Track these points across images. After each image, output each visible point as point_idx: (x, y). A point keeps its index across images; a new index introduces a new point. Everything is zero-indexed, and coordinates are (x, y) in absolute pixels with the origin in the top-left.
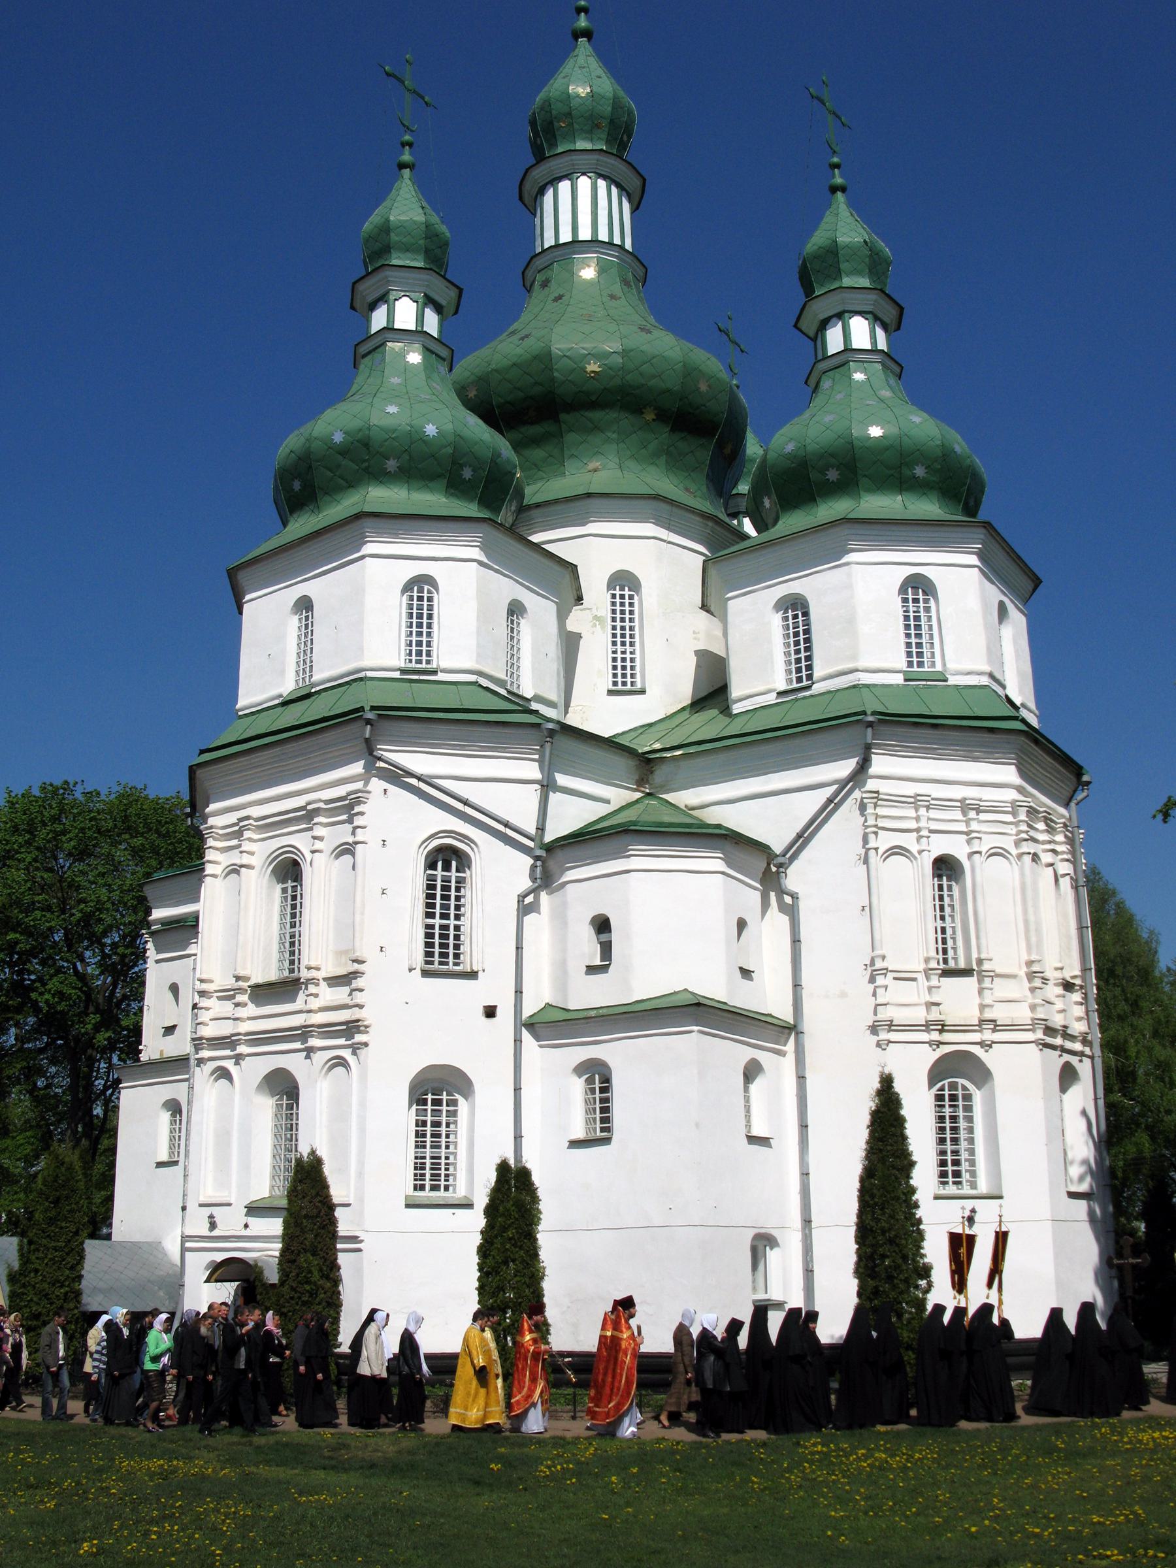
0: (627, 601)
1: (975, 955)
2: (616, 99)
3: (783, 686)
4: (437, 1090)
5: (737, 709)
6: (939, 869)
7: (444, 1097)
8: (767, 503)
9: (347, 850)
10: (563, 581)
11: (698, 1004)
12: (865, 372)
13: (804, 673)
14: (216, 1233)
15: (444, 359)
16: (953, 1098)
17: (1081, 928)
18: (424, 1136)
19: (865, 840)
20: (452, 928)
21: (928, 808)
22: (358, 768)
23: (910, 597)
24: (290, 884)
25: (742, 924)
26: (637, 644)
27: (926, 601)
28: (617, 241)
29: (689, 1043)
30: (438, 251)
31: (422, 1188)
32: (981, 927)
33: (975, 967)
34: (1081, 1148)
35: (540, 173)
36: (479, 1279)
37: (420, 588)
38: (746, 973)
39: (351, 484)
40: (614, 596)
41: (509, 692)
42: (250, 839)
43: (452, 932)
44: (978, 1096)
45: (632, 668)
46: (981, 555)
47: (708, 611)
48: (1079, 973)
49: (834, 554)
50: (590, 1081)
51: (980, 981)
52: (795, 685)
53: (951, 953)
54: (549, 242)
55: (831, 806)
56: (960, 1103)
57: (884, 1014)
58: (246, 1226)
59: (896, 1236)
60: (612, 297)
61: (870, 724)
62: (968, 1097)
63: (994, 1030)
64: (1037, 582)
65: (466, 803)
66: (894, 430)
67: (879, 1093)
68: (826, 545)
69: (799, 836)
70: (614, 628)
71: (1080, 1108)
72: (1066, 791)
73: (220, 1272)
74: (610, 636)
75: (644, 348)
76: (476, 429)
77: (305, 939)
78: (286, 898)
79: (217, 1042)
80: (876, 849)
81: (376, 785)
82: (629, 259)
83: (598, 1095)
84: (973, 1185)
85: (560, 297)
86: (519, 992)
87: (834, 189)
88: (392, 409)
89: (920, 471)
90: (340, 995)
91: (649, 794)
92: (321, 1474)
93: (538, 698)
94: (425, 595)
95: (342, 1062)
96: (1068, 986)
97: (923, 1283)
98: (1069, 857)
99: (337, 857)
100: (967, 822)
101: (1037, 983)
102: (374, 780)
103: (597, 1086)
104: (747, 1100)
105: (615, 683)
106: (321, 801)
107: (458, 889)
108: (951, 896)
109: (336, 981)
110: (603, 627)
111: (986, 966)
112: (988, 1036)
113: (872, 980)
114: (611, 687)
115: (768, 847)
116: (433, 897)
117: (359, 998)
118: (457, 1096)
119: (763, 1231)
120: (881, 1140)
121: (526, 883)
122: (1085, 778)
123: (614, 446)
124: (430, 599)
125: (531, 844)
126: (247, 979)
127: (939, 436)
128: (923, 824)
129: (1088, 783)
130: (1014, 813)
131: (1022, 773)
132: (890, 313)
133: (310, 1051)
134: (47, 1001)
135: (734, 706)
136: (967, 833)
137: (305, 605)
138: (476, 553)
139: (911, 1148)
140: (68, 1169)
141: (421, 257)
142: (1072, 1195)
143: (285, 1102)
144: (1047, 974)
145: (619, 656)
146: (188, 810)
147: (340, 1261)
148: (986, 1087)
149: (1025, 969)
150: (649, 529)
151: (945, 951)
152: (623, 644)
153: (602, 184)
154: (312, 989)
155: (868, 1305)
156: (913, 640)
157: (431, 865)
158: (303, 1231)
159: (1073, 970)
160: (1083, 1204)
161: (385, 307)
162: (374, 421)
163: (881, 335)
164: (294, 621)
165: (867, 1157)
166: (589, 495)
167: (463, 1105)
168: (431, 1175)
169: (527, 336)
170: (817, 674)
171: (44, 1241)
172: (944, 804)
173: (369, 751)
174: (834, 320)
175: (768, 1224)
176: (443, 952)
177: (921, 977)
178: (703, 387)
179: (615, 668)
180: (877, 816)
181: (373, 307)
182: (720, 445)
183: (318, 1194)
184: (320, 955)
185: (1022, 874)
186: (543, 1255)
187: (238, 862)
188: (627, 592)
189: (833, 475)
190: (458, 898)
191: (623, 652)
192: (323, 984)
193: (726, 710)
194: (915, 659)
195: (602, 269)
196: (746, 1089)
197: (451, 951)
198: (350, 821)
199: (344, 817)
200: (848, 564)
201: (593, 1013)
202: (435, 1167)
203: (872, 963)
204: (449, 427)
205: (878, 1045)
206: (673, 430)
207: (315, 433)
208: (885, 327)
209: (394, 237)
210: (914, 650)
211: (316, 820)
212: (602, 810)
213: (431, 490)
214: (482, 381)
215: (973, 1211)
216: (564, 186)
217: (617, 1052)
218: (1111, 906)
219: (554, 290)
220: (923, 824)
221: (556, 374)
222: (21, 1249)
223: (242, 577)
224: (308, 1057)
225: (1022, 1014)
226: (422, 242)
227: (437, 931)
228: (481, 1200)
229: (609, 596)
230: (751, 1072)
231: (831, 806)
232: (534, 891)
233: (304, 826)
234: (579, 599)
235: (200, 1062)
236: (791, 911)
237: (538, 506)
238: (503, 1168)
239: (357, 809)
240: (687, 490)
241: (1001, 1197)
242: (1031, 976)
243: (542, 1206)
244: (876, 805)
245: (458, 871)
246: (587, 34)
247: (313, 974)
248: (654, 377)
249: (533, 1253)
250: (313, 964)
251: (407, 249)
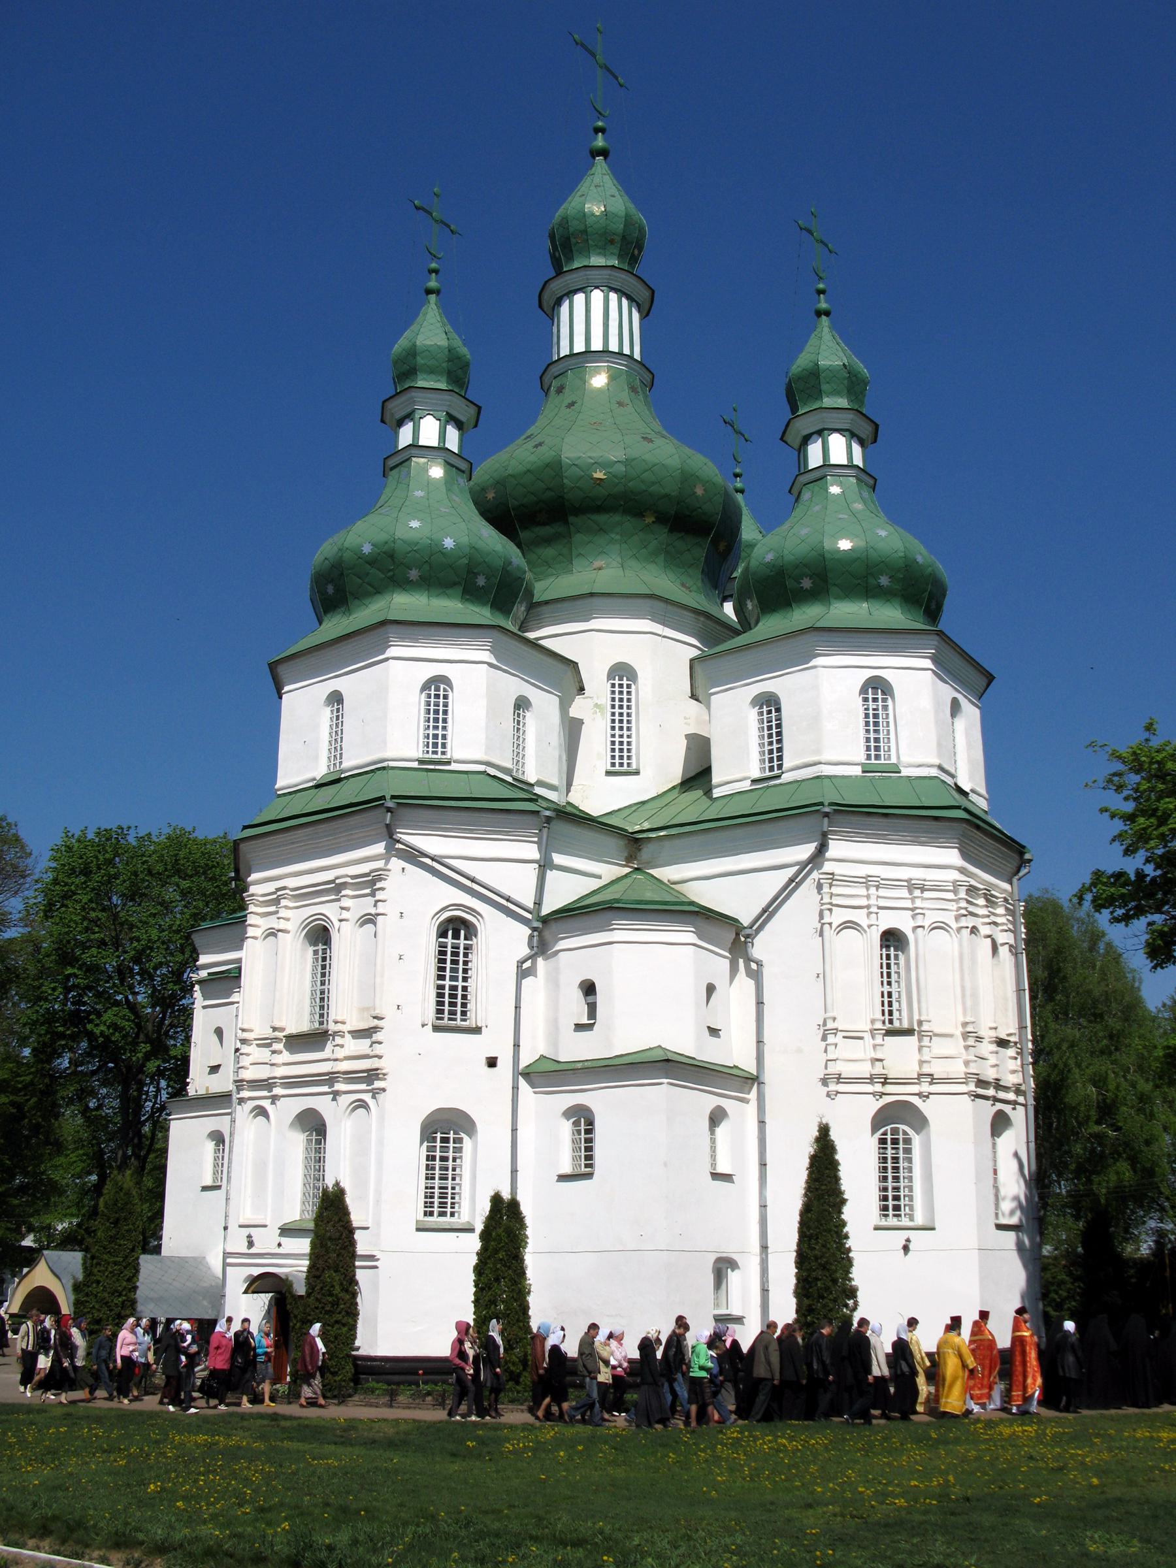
0: (625, 690)
1: (916, 1017)
2: (628, 216)
3: (757, 774)
4: (445, 1130)
5: (717, 793)
6: (887, 940)
7: (452, 1136)
8: (750, 605)
9: (369, 920)
10: (565, 676)
11: (668, 1060)
12: (840, 485)
13: (775, 763)
15: (463, 472)
16: (895, 1142)
17: (1020, 991)
18: (433, 1169)
19: (821, 916)
20: (460, 989)
21: (878, 887)
22: (379, 848)
23: (870, 696)
24: (321, 947)
25: (711, 989)
26: (634, 729)
27: (884, 700)
28: (627, 351)
29: (660, 1094)
30: (460, 372)
31: (431, 1214)
32: (923, 992)
33: (916, 1027)
34: (1013, 1186)
35: (557, 286)
36: (475, 1294)
37: (437, 687)
38: (714, 1032)
39: (378, 590)
40: (613, 685)
41: (514, 779)
42: (286, 907)
43: (460, 992)
44: (917, 1140)
45: (629, 750)
46: (934, 659)
47: (697, 700)
48: (1017, 1031)
49: (803, 658)
50: (576, 1123)
51: (920, 1040)
52: (768, 774)
53: (896, 1015)
54: (564, 351)
55: (793, 885)
56: (901, 1146)
57: (834, 1069)
58: (279, 1245)
59: (827, 1262)
60: (620, 404)
61: (826, 815)
62: (908, 1141)
63: (931, 1083)
64: (990, 678)
65: (473, 880)
66: (862, 544)
67: (818, 1140)
68: (798, 649)
69: (764, 911)
70: (613, 714)
71: (1013, 1151)
72: (1011, 867)
73: (256, 1285)
74: (609, 721)
75: (647, 457)
76: (491, 540)
77: (333, 996)
78: (317, 959)
79: (256, 1084)
80: (830, 924)
81: (396, 864)
82: (637, 367)
83: (583, 1136)
84: (912, 1219)
85: (572, 404)
86: (517, 1046)
87: (819, 313)
88: (415, 524)
89: (884, 581)
90: (363, 1046)
91: (637, 869)
92: (332, 1448)
93: (540, 783)
94: (442, 693)
95: (363, 1105)
96: (1002, 1043)
97: (851, 1302)
98: (1011, 927)
99: (362, 925)
100: (913, 899)
101: (971, 1042)
102: (394, 859)
103: (583, 1128)
104: (713, 1141)
105: (613, 765)
106: (348, 876)
107: (466, 955)
108: (897, 964)
109: (358, 1034)
110: (602, 714)
111: (925, 1027)
112: (925, 1088)
113: (824, 1038)
114: (609, 768)
115: (736, 920)
116: (444, 961)
117: (378, 1049)
118: (463, 1135)
119: (724, 1255)
120: (816, 1180)
121: (525, 951)
122: (1027, 856)
123: (618, 546)
124: (446, 697)
125: (529, 916)
126: (282, 1030)
127: (902, 549)
128: (873, 901)
129: (1030, 861)
130: (955, 892)
131: (965, 855)
132: (865, 430)
133: (336, 1094)
134: (102, 1033)
135: (714, 791)
136: (912, 910)
137: (336, 699)
138: (486, 656)
139: (843, 1188)
140: (126, 1194)
141: (444, 379)
142: (1000, 1227)
143: (314, 1137)
144: (982, 1033)
145: (617, 739)
146: (233, 874)
147: (358, 1277)
148: (924, 1132)
149: (961, 1029)
151: (891, 1013)
152: (621, 728)
153: (613, 296)
154: (338, 1040)
155: (803, 1320)
156: (872, 736)
157: (442, 934)
158: (327, 1251)
159: (1009, 1027)
160: (1011, 1236)
161: (411, 424)
162: (400, 533)
163: (857, 449)
164: (327, 712)
165: (806, 1195)
166: (592, 595)
167: (467, 1143)
168: (439, 1201)
169: (540, 444)
170: (786, 766)
171: (105, 1257)
172: (893, 883)
173: (390, 834)
174: (815, 436)
175: (729, 1249)
176: (452, 1009)
177: (867, 1036)
178: (699, 491)
179: (613, 750)
180: (832, 895)
181: (400, 423)
182: (715, 543)
183: (340, 1220)
184: (346, 1011)
185: (961, 945)
186: (529, 1273)
187: (276, 926)
188: (625, 682)
189: (807, 583)
190: (466, 963)
191: (621, 736)
192: (348, 1036)
193: (708, 792)
194: (873, 753)
195: (612, 378)
196: (712, 1132)
197: (459, 1009)
198: (373, 894)
199: (368, 891)
200: (815, 667)
201: (579, 1065)
202: (443, 1196)
203: (825, 1024)
204: (465, 540)
205: (828, 1095)
206: (671, 531)
207: (346, 545)
208: (862, 443)
209: (420, 361)
210: (872, 744)
211: (344, 893)
212: (595, 884)
213: (449, 596)
214: (500, 484)
215: (908, 1240)
216: (579, 298)
217: (601, 1100)
218: (1102, 947)
219: (567, 396)
220: (873, 898)
221: (565, 481)
222: (84, 1264)
223: (282, 670)
224: (334, 1099)
225: (957, 1069)
226: (445, 365)
227: (447, 992)
228: (479, 1227)
229: (609, 685)
230: (716, 1118)
231: (793, 885)
232: (532, 957)
233: (333, 897)
234: (582, 689)
235: (241, 1101)
236: (756, 975)
237: (547, 603)
238: (496, 1199)
239: (378, 885)
240: (683, 585)
241: (933, 1229)
242: (966, 1035)
243: (529, 1232)
244: (831, 885)
245: (466, 939)
246: (604, 153)
247: (339, 1027)
248: (653, 483)
249: (521, 1273)
250: (339, 1018)
251: (432, 371)
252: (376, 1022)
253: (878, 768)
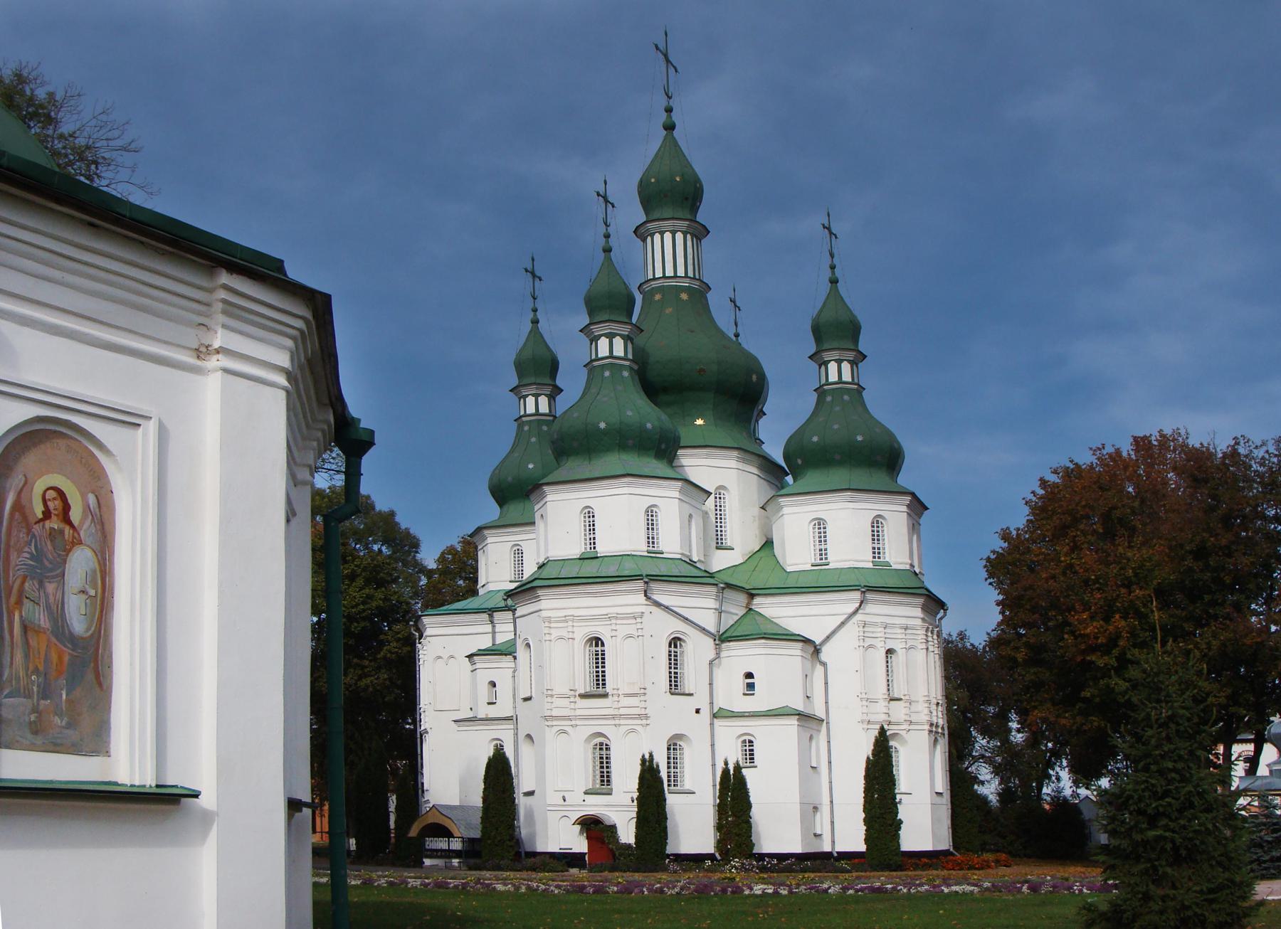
86: (712, 703)
95: (633, 731)
150: (733, 464)
176: (675, 685)
253: (881, 566)
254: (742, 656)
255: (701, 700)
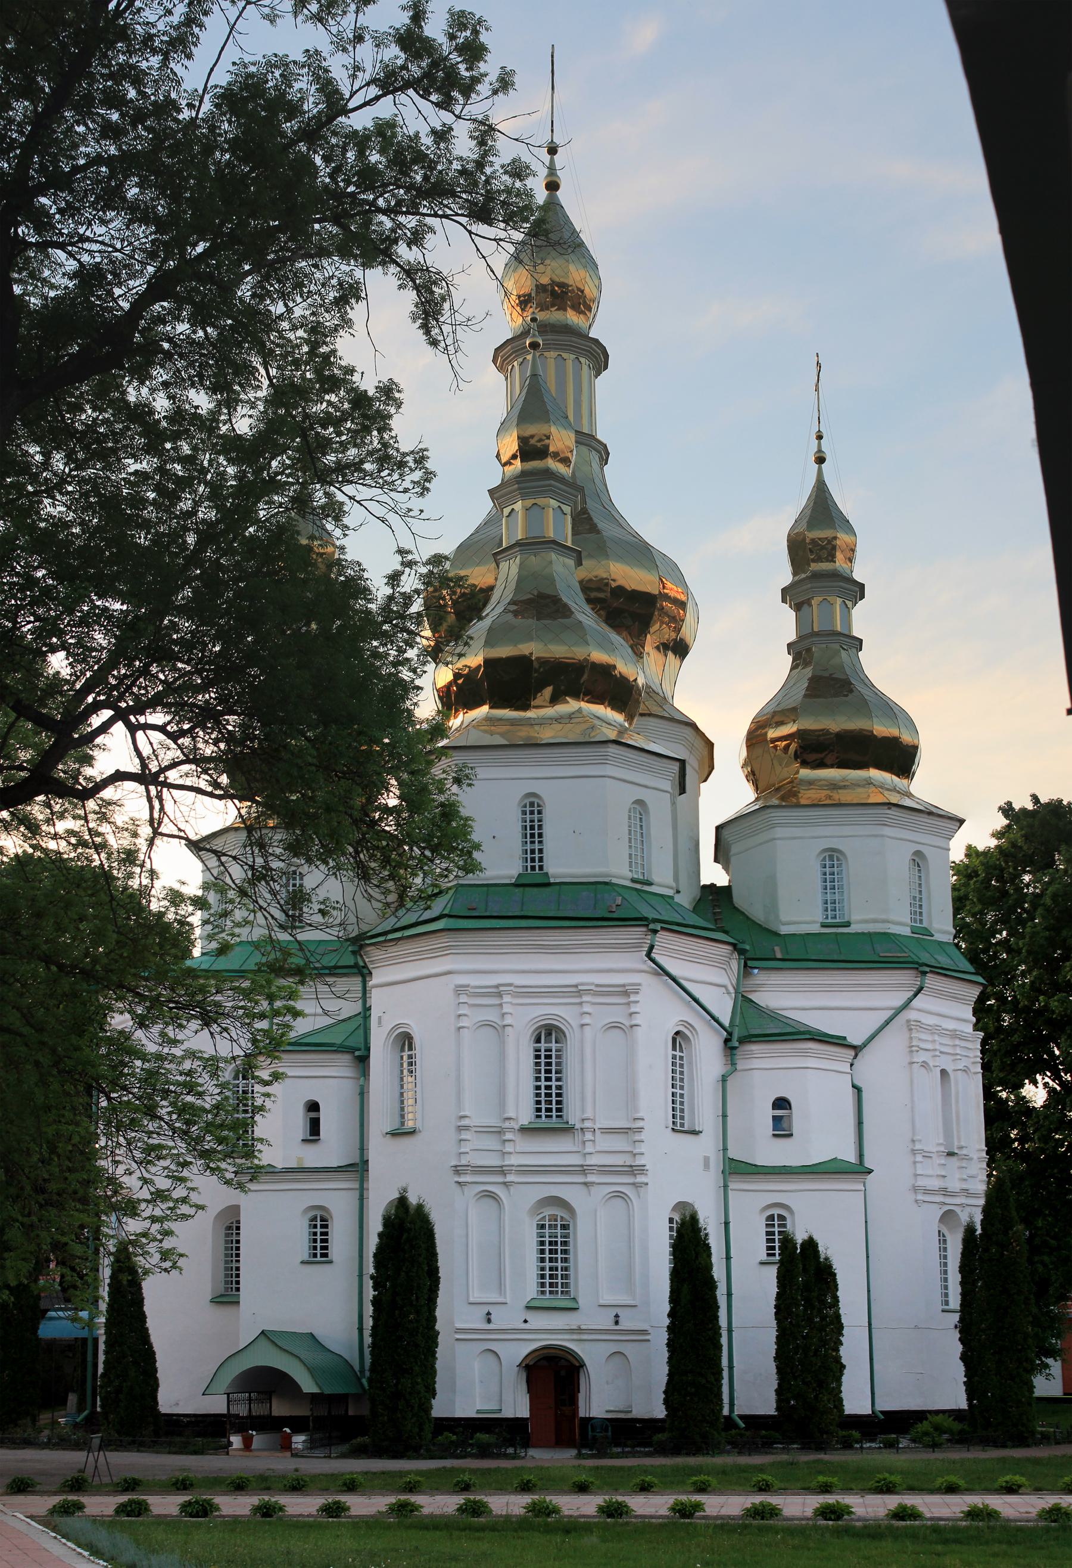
1: (956, 1144)
14: (491, 1326)
90: (619, 1143)
95: (620, 1196)
106: (592, 984)
198: (628, 1004)
200: (882, 836)
252: (640, 1124)
254: (770, 1070)
255: (707, 1145)
